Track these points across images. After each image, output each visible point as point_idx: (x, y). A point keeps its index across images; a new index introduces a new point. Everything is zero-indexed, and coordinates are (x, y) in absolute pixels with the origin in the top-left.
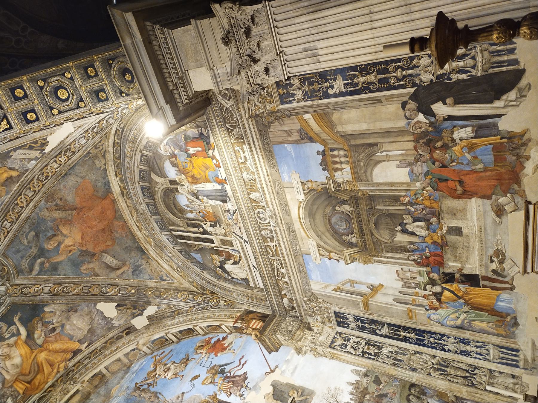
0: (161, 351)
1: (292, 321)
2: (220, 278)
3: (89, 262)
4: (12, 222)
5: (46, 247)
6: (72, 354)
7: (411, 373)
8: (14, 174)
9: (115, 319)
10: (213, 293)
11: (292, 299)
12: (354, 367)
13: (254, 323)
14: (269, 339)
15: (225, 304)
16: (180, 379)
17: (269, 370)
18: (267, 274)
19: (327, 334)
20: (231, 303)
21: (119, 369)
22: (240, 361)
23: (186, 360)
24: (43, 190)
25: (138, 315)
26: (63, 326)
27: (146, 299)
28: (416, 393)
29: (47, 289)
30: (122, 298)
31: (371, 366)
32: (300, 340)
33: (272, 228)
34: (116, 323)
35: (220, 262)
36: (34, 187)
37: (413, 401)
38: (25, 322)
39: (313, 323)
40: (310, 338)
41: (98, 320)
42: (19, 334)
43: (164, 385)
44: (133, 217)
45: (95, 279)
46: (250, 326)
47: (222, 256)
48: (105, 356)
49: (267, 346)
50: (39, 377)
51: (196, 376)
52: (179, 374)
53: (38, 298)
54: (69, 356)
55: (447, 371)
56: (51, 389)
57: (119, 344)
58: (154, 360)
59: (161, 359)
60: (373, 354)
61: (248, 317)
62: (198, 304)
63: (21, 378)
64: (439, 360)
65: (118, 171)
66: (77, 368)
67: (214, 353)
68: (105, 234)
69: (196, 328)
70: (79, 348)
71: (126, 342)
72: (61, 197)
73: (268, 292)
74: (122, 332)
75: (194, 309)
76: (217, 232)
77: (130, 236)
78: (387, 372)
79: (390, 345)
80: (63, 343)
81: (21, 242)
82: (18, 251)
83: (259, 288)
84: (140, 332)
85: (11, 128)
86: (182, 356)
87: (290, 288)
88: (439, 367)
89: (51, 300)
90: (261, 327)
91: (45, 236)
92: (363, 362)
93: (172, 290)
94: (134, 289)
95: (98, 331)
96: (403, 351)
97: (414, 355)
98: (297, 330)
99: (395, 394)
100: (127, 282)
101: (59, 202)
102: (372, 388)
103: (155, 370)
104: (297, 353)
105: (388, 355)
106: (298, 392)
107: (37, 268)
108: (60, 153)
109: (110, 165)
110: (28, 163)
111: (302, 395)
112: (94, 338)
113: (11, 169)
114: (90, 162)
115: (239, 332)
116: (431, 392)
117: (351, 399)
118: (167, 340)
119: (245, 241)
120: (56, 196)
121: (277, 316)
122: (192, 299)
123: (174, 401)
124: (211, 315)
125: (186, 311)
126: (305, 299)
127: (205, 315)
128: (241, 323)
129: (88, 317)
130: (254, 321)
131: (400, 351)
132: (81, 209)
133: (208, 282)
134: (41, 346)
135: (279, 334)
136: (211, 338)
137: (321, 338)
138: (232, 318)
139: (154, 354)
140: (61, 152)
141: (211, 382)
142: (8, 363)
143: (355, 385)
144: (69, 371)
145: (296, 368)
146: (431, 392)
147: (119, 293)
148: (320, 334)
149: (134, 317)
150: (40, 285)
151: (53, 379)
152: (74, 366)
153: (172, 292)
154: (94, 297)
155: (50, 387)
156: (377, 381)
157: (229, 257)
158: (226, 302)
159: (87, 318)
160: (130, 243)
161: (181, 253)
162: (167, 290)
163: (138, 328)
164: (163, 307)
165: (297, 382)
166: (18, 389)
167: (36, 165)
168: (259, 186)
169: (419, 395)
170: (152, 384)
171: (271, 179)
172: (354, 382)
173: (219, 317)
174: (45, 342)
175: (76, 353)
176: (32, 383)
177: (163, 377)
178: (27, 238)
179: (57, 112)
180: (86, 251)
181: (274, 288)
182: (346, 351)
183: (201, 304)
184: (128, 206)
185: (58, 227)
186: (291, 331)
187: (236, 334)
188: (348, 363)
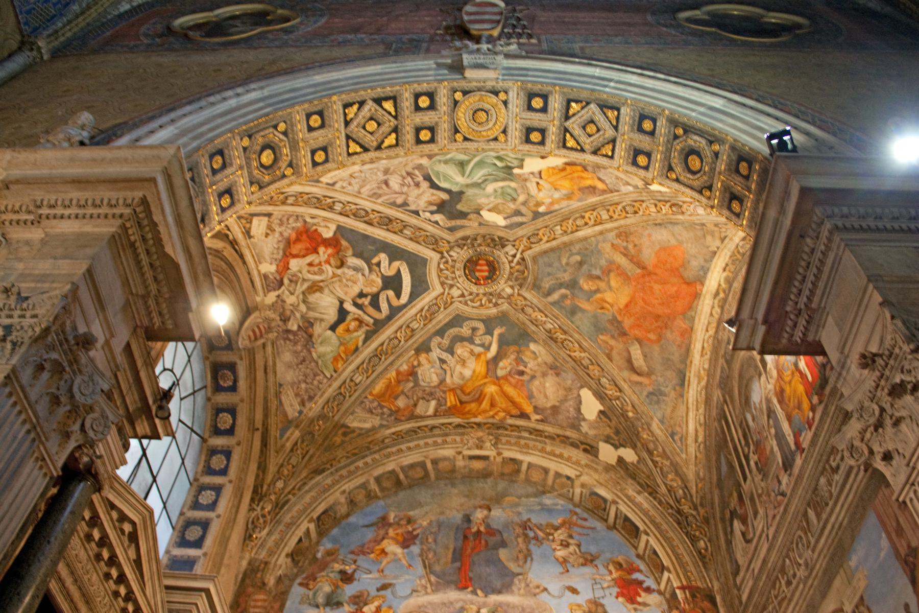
0: (585, 515)
2: (723, 520)
3: (613, 337)
4: (565, 232)
5: (581, 282)
8: (600, 186)
16: (561, 570)
21: (535, 483)
23: (589, 560)
24: (622, 222)
25: (612, 445)
26: (533, 377)
29: (549, 326)
30: (612, 408)
33: (798, 574)
34: (585, 427)
36: (614, 212)
38: (502, 342)
42: (488, 348)
44: (707, 331)
45: (603, 360)
48: (543, 450)
50: (473, 405)
52: (568, 565)
53: (533, 328)
54: (515, 412)
59: (576, 525)
62: (679, 512)
63: (459, 392)
65: (730, 266)
66: (512, 431)
67: (618, 590)
68: (657, 321)
71: (574, 459)
72: (637, 243)
74: (582, 443)
75: (670, 511)
76: (756, 479)
77: (683, 350)
80: (519, 395)
81: (559, 259)
82: (550, 265)
83: (741, 596)
84: (597, 464)
85: (612, 157)
86: (593, 549)
89: (544, 341)
91: (589, 271)
95: (561, 417)
100: (634, 398)
101: (630, 246)
103: (557, 529)
107: (555, 296)
108: (667, 202)
109: (724, 253)
110: (624, 185)
112: (551, 419)
113: (599, 179)
114: (700, 233)
118: (605, 510)
119: (767, 536)
120: (631, 238)
122: (678, 497)
123: (531, 585)
124: (676, 542)
125: (660, 501)
127: (671, 534)
128: (686, 597)
129: (564, 393)
132: (650, 274)
134: (498, 378)
138: (688, 578)
139: (578, 510)
140: (669, 201)
142: (458, 368)
149: (606, 442)
150: (546, 316)
152: (511, 426)
153: (668, 463)
154: (587, 378)
155: (475, 423)
157: (744, 521)
158: (706, 550)
159: (562, 392)
160: (676, 357)
162: (664, 455)
164: (642, 466)
166: (448, 400)
167: (631, 193)
168: (824, 516)
171: (840, 533)
173: (677, 557)
174: (505, 378)
175: (523, 415)
176: (464, 405)
177: (554, 547)
178: (569, 258)
179: (674, 176)
180: (619, 322)
183: (681, 516)
184: (711, 314)
185: (610, 271)
187: (664, 602)
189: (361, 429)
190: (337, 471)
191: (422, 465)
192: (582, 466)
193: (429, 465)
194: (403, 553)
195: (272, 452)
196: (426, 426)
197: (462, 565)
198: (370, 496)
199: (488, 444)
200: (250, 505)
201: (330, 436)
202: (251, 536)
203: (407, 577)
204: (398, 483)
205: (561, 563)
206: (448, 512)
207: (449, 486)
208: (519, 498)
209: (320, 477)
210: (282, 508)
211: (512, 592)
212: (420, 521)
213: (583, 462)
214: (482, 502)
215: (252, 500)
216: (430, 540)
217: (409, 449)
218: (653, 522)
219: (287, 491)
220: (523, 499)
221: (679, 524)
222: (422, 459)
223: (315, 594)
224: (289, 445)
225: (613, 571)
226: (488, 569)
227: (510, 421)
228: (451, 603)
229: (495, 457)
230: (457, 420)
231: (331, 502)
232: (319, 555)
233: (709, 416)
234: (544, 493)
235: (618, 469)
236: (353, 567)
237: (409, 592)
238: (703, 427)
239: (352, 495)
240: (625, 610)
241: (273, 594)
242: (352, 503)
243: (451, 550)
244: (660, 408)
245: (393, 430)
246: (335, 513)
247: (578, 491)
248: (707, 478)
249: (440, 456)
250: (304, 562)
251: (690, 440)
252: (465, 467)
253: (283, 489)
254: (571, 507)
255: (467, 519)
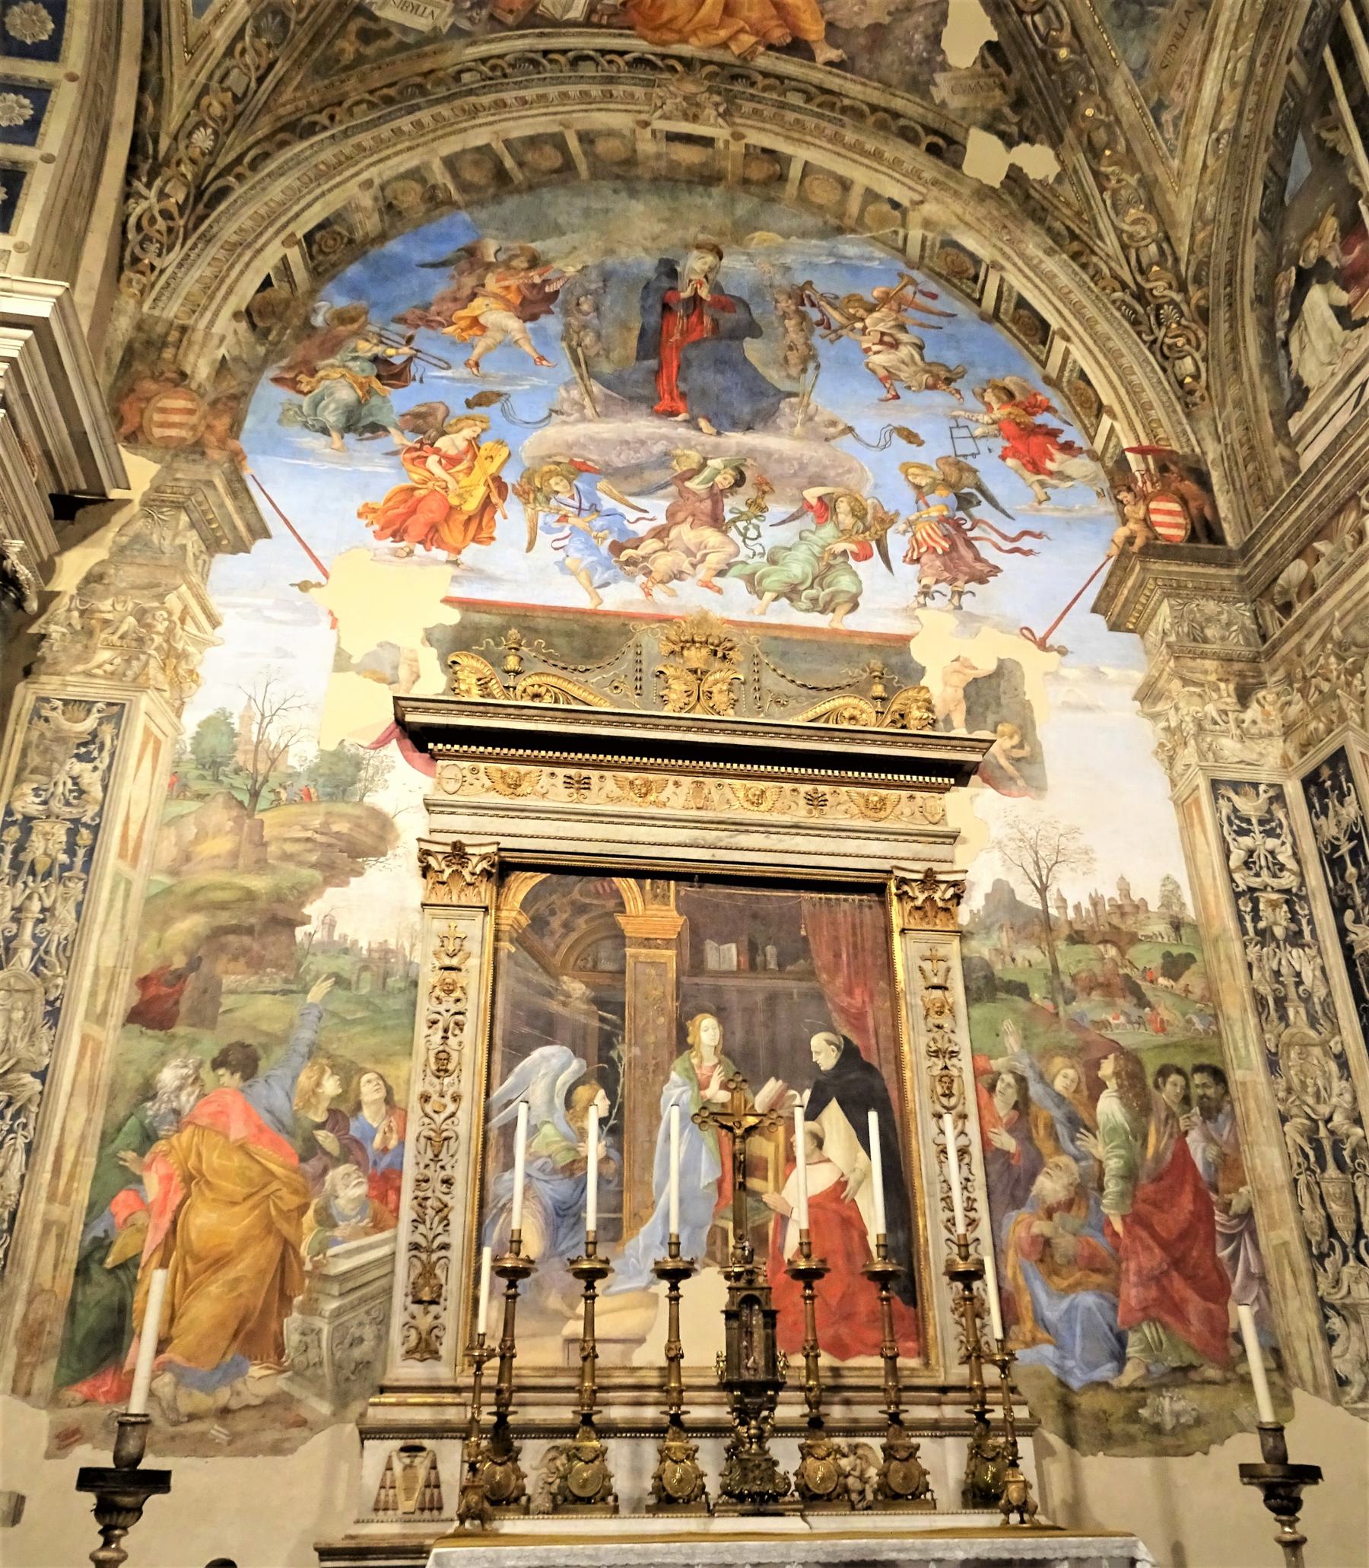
0: (933, 287)
1: (1243, 628)
2: (1265, 300)
6: (789, 40)
7: (1257, 1059)
9: (949, 75)
10: (1204, 315)
11: (1313, 590)
12: (1182, 878)
13: (1170, 513)
14: (1141, 585)
15: (1188, 380)
16: (884, 394)
17: (1039, 634)
18: (1360, 450)
19: (1255, 756)
20: (1202, 398)
21: (821, 207)
22: (1025, 533)
23: (944, 379)
25: (1003, 136)
27: (1063, 117)
28: (1200, 1091)
31: (1215, 930)
32: (1186, 682)
34: (942, 88)
35: (1322, 261)
37: (1168, 1086)
39: (1270, 698)
40: (1211, 709)
41: (917, 27)
43: (845, 364)
46: (1153, 505)
47: (1346, 249)
48: (836, 139)
49: (1112, 590)
51: (916, 436)
54: (779, 35)
55: (1323, 1169)
56: (679, 67)
57: (895, 149)
58: (897, 285)
60: (1262, 925)
61: (1182, 480)
62: (1140, 295)
64: (1353, 1140)
66: (765, 89)
67: (1007, 444)
69: (1057, 339)
70: (814, 46)
71: (908, 166)
73: (1295, 495)
74: (929, 130)
75: (1118, 295)
78: (1223, 987)
79: (1323, 969)
83: (1297, 456)
84: (958, 182)
87: (1348, 561)
88: (1327, 1145)
90: (1167, 538)
92: (1218, 903)
93: (1137, 176)
94: (1073, 51)
95: (888, 57)
96: (1323, 1016)
97: (1326, 1053)
98: (1219, 658)
99: (1163, 1030)
102: (1146, 957)
103: (871, 309)
104: (1140, 690)
105: (1284, 971)
106: (1021, 746)
111: (1017, 761)
112: (863, 62)
115: (1112, 480)
116: (1226, 1133)
117: (1077, 908)
118: (975, 279)
121: (1237, 571)
124: (1128, 360)
126: (1337, 632)
127: (1116, 343)
128: (1148, 470)
130: (1176, 507)
131: (1318, 1008)
133: (1231, 273)
135: (1171, 607)
136: (1049, 409)
137: (1229, 746)
138: (1152, 433)
139: (917, 275)
141: (918, 487)
143: (1126, 902)
144: (745, 72)
145: (1088, 708)
146: (1226, 1133)
147: (1033, 14)
148: (1244, 736)
149: (988, 128)
151: (701, 48)
152: (766, 75)
153: (1133, 181)
155: (680, 59)
156: (1175, 966)
158: (1196, 377)
161: (1283, 100)
163: (966, 168)
164: (1067, 191)
165: (1048, 732)
169: (1194, 1101)
170: (829, 327)
172: (1136, 897)
173: (1133, 391)
175: (799, 48)
181: (1321, 508)
182: (1229, 839)
186: (1205, 641)
187: (1102, 474)
188: (1191, 859)
189: (405, 30)
190: (346, 134)
191: (558, 141)
192: (925, 184)
193: (574, 145)
194: (524, 331)
195: (177, 49)
196: (564, 52)
197: (661, 366)
198: (435, 200)
199: (710, 112)
200: (128, 183)
201: (330, 32)
202: (136, 260)
203: (536, 381)
204: (501, 176)
205: (882, 380)
206: (623, 250)
207: (624, 194)
208: (786, 235)
209: (306, 144)
210: (211, 206)
211: (777, 430)
212: (555, 265)
213: (927, 175)
214: (701, 237)
215: (131, 170)
216: (585, 307)
217: (524, 102)
218: (1078, 311)
219: (223, 161)
220: (793, 239)
221: (1135, 323)
222: (555, 129)
223: (316, 405)
224: (221, 36)
225: (995, 406)
226: (719, 377)
227: (765, 61)
228: (643, 443)
229: (727, 142)
230: (638, 45)
231: (339, 206)
232: (318, 321)
233: (1269, 57)
234: (840, 230)
235: (1006, 197)
236: (406, 350)
237: (546, 413)
238: (1239, 91)
239: (388, 192)
240: (1020, 483)
241: (211, 396)
242: (390, 209)
243: (637, 332)
244: (1143, 37)
245: (483, 50)
246: (351, 230)
247: (916, 234)
248: (1225, 218)
249: (598, 126)
250: (281, 334)
251: (1200, 122)
252: (659, 156)
253: (214, 153)
254: (901, 266)
255: (669, 270)
